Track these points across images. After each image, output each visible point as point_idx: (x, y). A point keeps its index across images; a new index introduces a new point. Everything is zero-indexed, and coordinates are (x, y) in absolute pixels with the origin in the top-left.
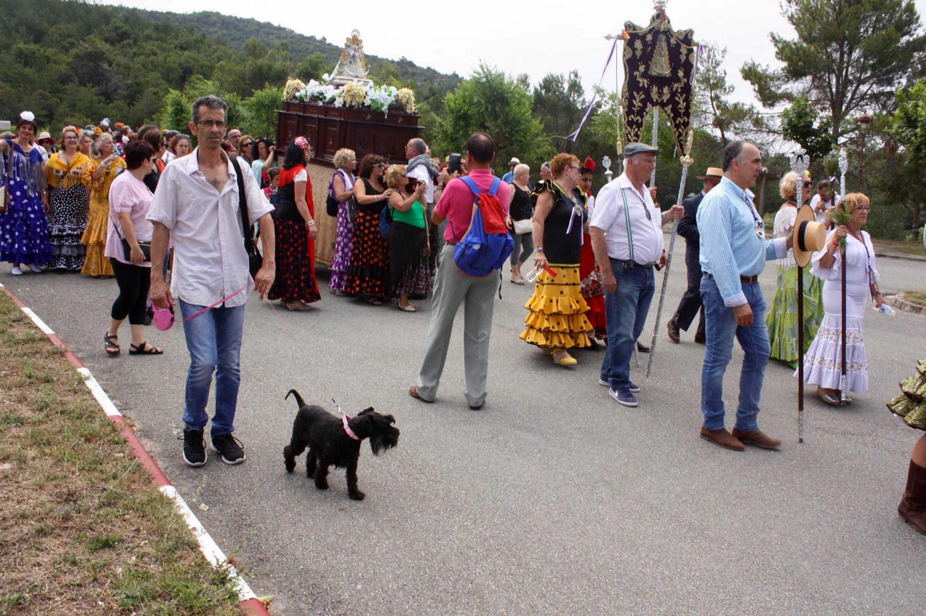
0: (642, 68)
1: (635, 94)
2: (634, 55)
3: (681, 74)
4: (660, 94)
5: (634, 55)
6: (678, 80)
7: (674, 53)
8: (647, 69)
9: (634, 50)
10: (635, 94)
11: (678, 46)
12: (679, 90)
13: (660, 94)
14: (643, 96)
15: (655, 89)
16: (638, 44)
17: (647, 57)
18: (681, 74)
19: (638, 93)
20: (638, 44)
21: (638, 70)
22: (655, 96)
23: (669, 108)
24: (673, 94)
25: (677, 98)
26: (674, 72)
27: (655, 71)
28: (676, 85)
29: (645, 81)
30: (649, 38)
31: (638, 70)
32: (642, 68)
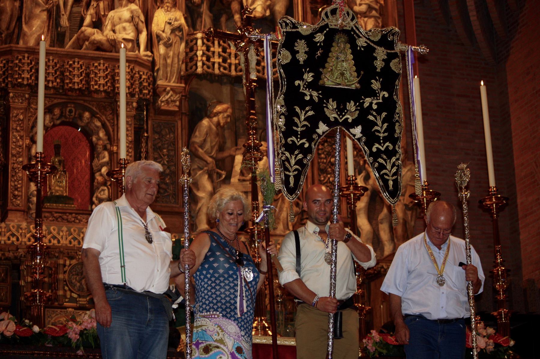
0: (309, 77)
1: (298, 109)
2: (294, 60)
3: (376, 85)
4: (341, 110)
5: (294, 60)
6: (373, 94)
7: (363, 59)
8: (318, 77)
9: (294, 53)
10: (298, 109)
11: (369, 50)
12: (375, 107)
13: (341, 110)
14: (311, 113)
15: (332, 105)
16: (301, 46)
17: (317, 62)
18: (376, 85)
19: (302, 108)
20: (301, 46)
21: (302, 79)
22: (332, 116)
23: (357, 131)
24: (364, 112)
25: (371, 118)
26: (365, 83)
27: (329, 81)
28: (368, 100)
29: (315, 94)
30: (320, 38)
31: (302, 79)
32: (309, 77)
